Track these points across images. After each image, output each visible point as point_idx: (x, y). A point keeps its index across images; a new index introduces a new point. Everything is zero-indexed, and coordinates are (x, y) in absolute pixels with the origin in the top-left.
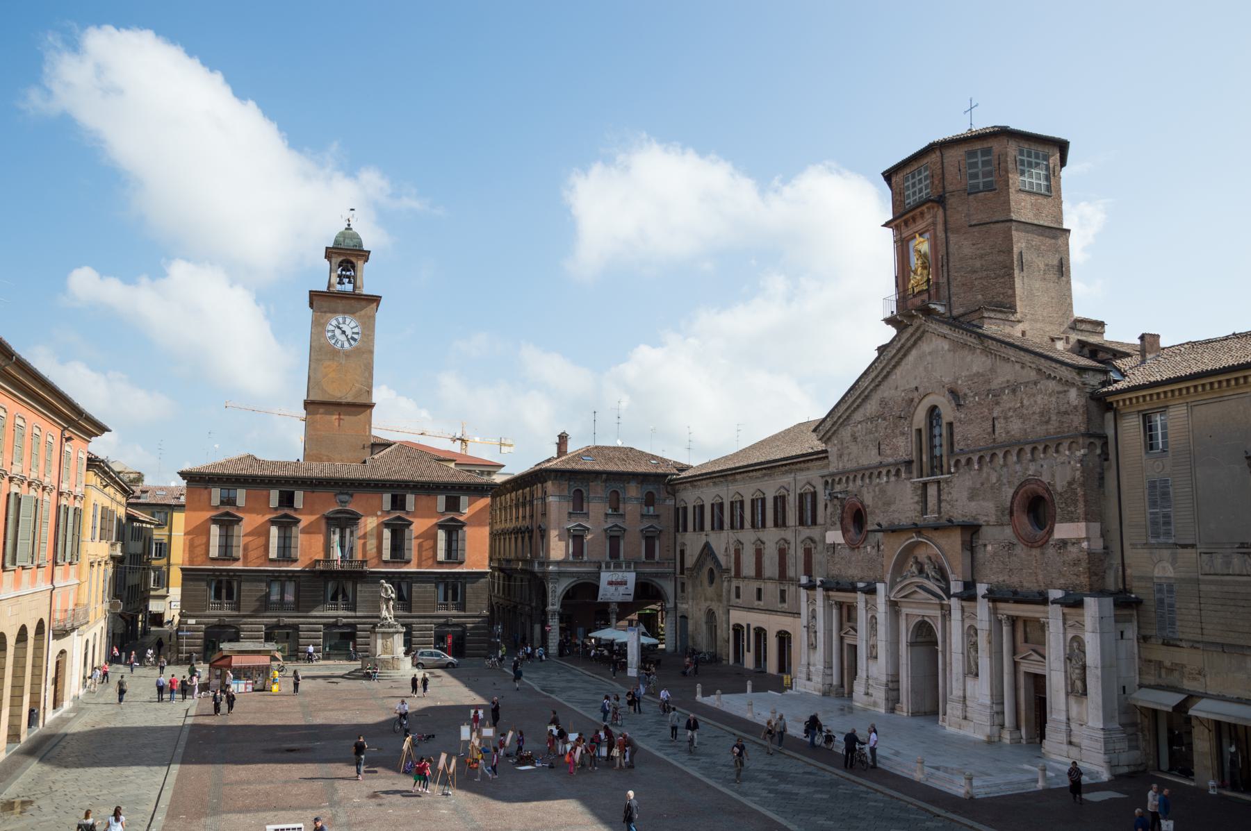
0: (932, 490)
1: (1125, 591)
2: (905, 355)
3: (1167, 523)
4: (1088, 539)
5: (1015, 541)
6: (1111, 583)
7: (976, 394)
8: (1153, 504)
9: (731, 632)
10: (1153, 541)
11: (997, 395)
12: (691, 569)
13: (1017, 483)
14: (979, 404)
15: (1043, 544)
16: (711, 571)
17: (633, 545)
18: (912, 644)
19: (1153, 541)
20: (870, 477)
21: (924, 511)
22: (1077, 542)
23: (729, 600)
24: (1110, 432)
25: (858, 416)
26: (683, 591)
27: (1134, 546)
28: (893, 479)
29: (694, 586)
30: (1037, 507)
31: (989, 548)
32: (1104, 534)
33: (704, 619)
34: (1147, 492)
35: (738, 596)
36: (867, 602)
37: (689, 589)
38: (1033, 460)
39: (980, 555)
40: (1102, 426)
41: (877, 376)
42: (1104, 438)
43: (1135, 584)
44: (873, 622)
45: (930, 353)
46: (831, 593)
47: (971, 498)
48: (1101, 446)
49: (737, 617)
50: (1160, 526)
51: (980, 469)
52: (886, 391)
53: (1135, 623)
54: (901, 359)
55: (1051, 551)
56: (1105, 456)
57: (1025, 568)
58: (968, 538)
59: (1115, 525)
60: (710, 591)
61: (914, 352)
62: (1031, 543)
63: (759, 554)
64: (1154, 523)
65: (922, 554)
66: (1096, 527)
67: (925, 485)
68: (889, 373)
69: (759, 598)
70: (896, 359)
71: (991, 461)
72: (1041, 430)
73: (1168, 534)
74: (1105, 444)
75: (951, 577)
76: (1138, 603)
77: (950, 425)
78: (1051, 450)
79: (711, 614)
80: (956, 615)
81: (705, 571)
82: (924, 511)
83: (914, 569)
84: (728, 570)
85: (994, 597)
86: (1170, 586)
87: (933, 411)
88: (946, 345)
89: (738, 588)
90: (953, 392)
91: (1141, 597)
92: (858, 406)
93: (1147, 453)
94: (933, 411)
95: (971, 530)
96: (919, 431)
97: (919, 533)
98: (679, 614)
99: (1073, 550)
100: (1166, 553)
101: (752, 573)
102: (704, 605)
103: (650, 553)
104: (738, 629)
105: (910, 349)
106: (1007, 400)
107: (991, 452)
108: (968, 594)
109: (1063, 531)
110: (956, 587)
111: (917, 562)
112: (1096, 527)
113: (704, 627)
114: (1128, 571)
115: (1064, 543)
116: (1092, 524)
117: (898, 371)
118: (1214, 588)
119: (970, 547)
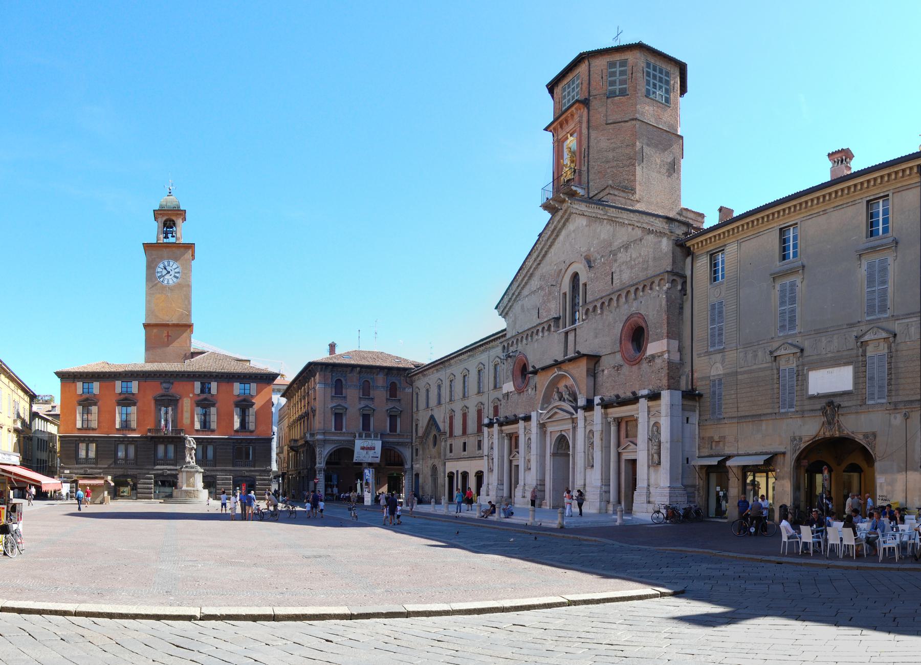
0: (571, 337)
1: (693, 390)
2: (557, 236)
3: (720, 335)
4: (669, 351)
5: (622, 363)
6: (684, 384)
7: (602, 256)
8: (713, 321)
9: (447, 479)
10: (712, 350)
11: (614, 253)
12: (422, 437)
13: (625, 318)
14: (604, 263)
16: (435, 436)
17: (380, 421)
18: (554, 455)
19: (712, 350)
20: (532, 336)
22: (662, 353)
23: (445, 455)
24: (688, 273)
25: (526, 292)
26: (417, 455)
27: (699, 355)
28: (546, 333)
29: (424, 449)
30: (637, 335)
31: (606, 372)
32: (680, 350)
33: (430, 473)
34: (709, 313)
35: (451, 452)
36: (525, 428)
37: (420, 452)
38: (635, 299)
39: (600, 379)
40: (683, 269)
41: (538, 256)
42: (684, 277)
43: (699, 384)
45: (574, 231)
46: (504, 428)
47: (596, 337)
48: (679, 279)
49: (451, 467)
50: (716, 337)
51: (602, 313)
52: (548, 267)
53: (697, 412)
54: (555, 239)
55: (645, 365)
56: (683, 291)
58: (592, 367)
59: (687, 343)
60: (433, 451)
61: (564, 233)
63: (465, 416)
64: (713, 336)
65: (561, 386)
66: (675, 343)
67: (567, 333)
68: (546, 252)
69: (464, 450)
70: (551, 240)
71: (609, 305)
72: (642, 276)
73: (720, 342)
74: (684, 283)
75: (579, 396)
76: (700, 396)
77: (585, 285)
78: (647, 290)
79: (434, 469)
80: (581, 423)
81: (431, 437)
82: (566, 354)
83: (556, 397)
84: (445, 433)
85: (605, 405)
86: (720, 380)
87: (576, 276)
89: (451, 445)
91: (702, 392)
92: (526, 283)
93: (711, 284)
94: (576, 276)
95: (594, 359)
96: (565, 294)
97: (560, 369)
98: (414, 473)
99: (658, 361)
100: (718, 357)
101: (461, 432)
102: (430, 463)
103: (393, 428)
104: (451, 476)
105: (561, 230)
106: (622, 256)
107: (608, 298)
108: (589, 406)
109: (652, 348)
110: (582, 402)
111: (558, 392)
112: (675, 343)
113: (430, 478)
114: (695, 375)
115: (653, 357)
116: (672, 341)
117: (552, 250)
118: (746, 376)
119: (593, 373)
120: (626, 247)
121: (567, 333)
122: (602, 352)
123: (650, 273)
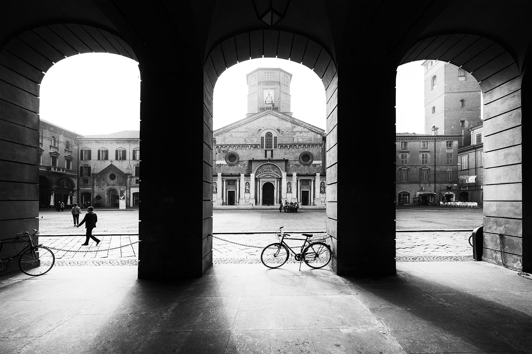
15: (309, 165)
21: (266, 156)
22: (319, 164)
25: (234, 130)
44: (248, 184)
57: (305, 170)
62: (305, 165)
72: (308, 142)
82: (266, 156)
88: (277, 118)
90: (279, 130)
95: (286, 161)
106: (298, 134)
109: (314, 162)
115: (316, 165)
120: (301, 132)
121: (266, 151)
122: (290, 160)
123: (313, 142)
